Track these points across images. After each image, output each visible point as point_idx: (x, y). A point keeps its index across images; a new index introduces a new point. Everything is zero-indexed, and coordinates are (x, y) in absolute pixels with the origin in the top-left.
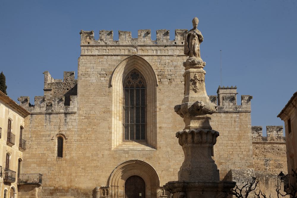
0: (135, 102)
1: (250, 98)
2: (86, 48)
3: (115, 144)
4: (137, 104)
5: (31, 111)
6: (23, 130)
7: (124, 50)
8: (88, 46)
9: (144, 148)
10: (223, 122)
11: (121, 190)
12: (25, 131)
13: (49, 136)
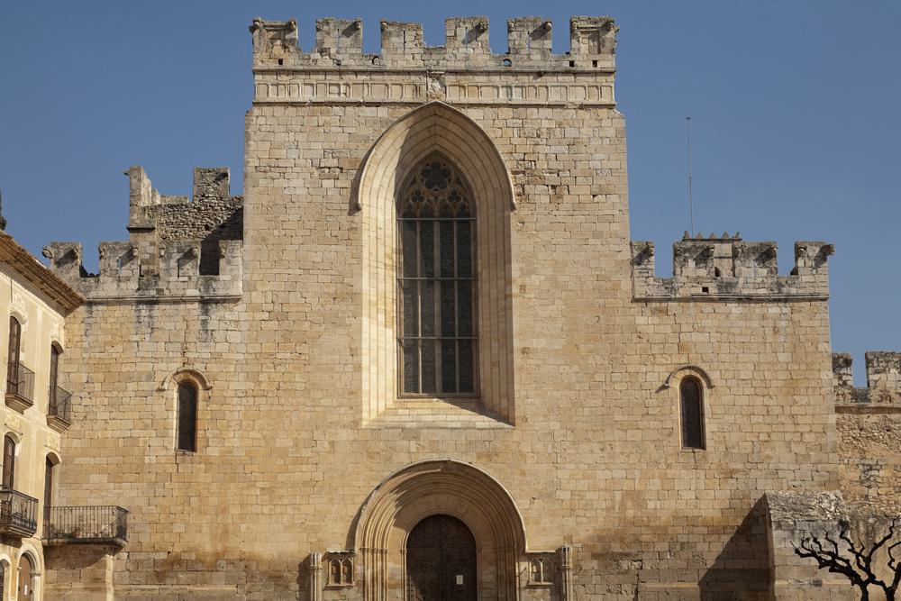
0: (437, 266)
1: (826, 251)
2: (270, 79)
3: (373, 407)
4: (444, 272)
5: (86, 292)
6: (61, 356)
7: (401, 85)
8: (277, 72)
9: (470, 422)
10: (737, 331)
11: (395, 565)
12: (69, 361)
13: (150, 377)
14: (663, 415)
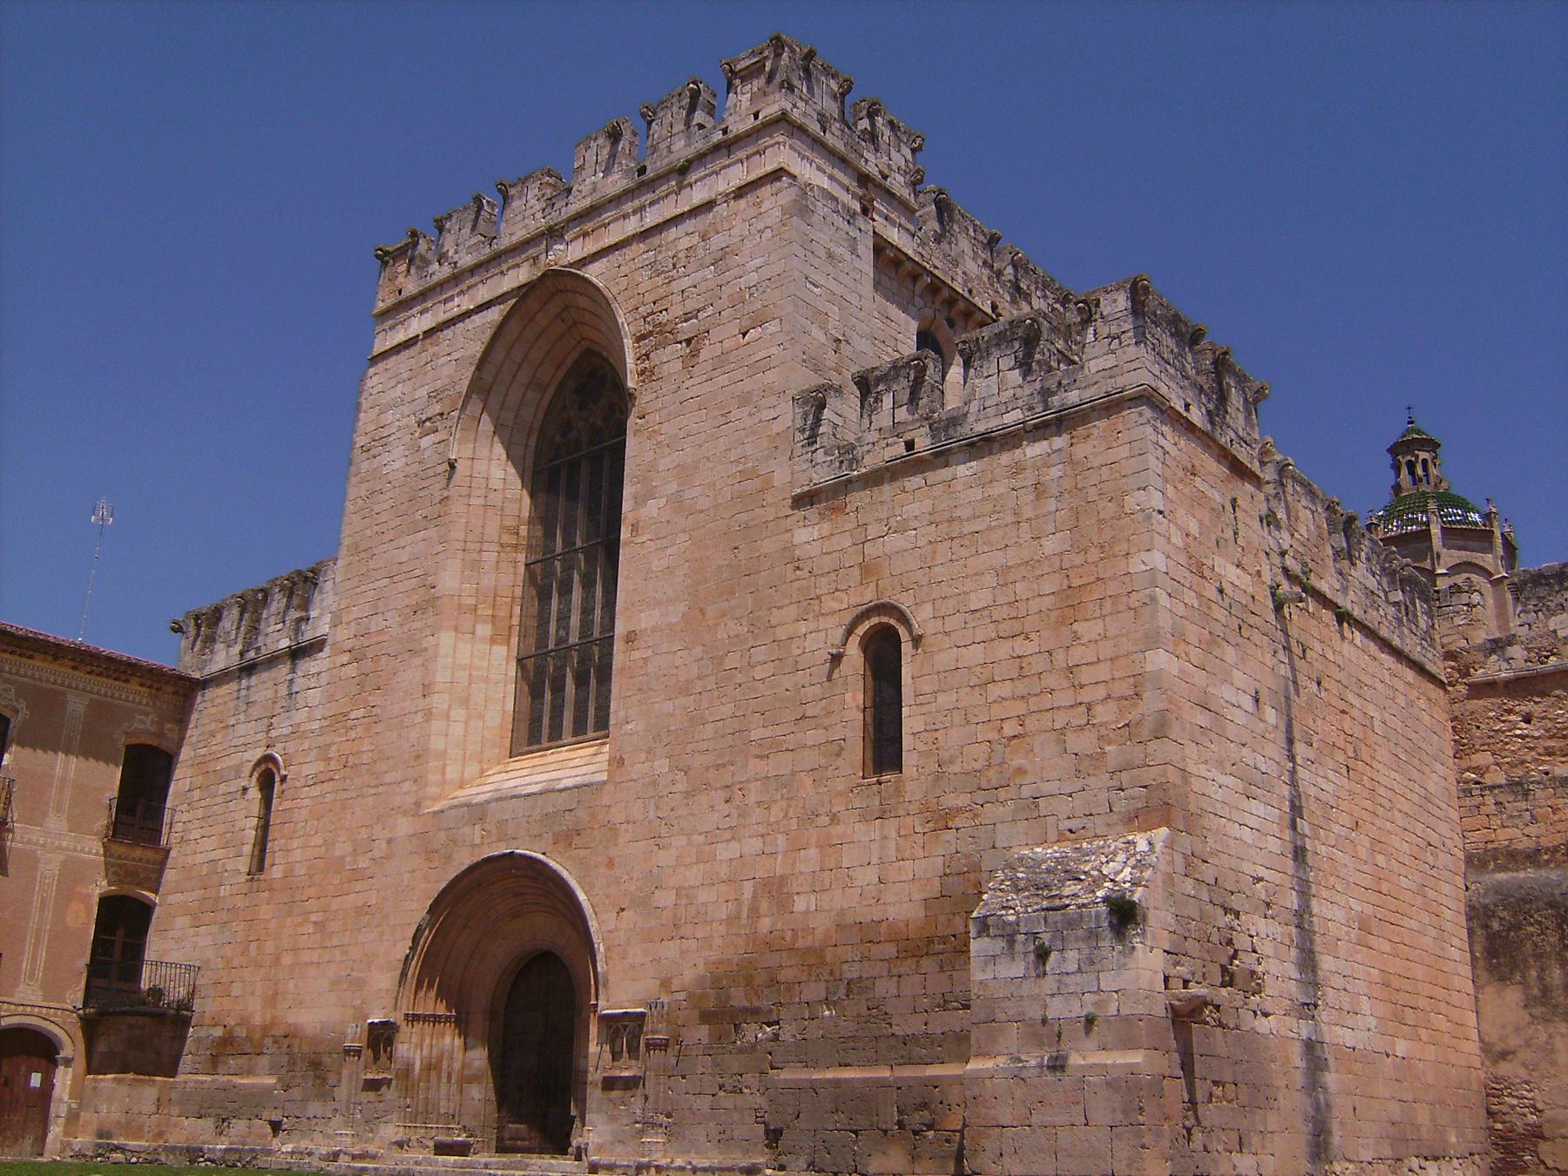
14: (829, 713)
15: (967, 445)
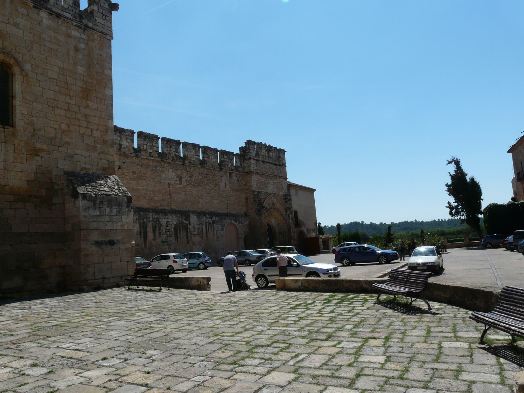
15: (49, 13)
